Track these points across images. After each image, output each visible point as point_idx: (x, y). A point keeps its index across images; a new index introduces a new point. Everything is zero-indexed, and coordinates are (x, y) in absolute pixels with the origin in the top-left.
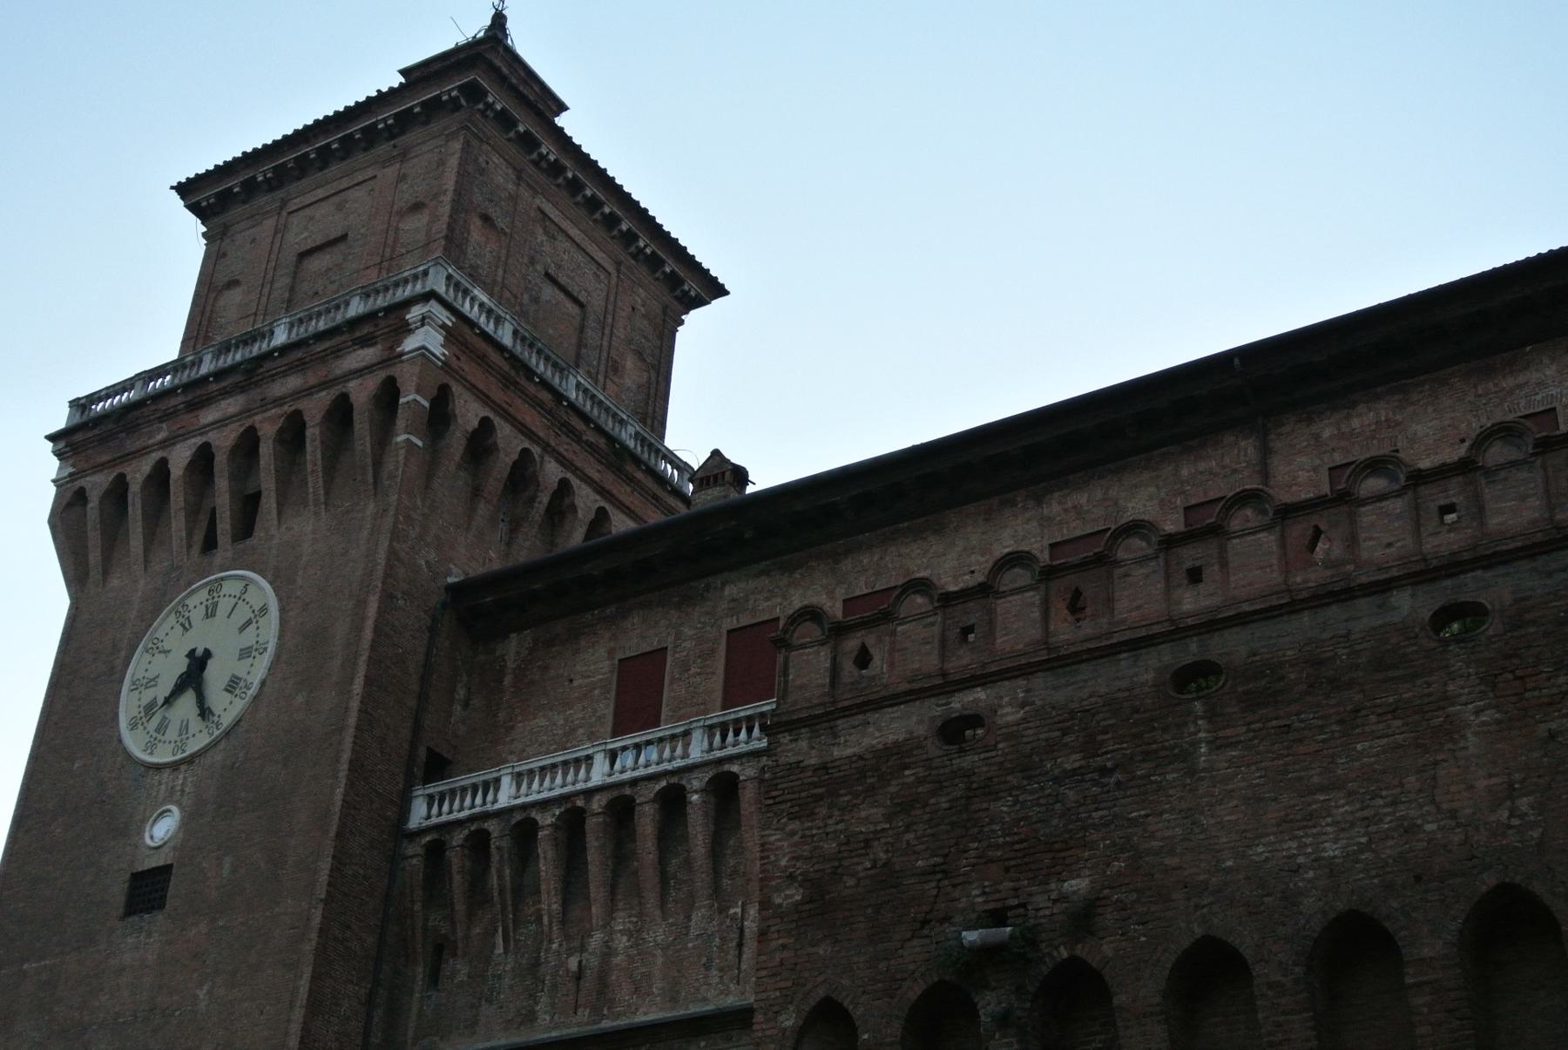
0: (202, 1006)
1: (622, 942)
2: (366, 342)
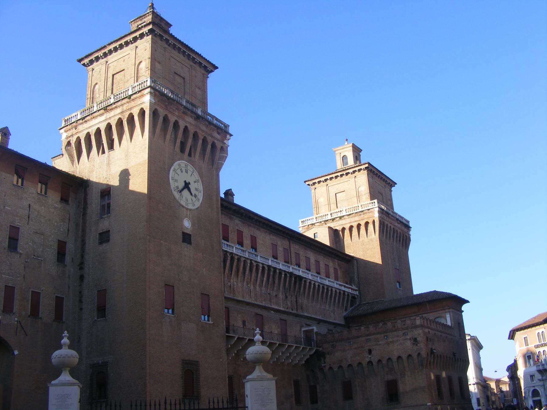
0: (205, 273)
1: (235, 283)
2: (219, 133)
